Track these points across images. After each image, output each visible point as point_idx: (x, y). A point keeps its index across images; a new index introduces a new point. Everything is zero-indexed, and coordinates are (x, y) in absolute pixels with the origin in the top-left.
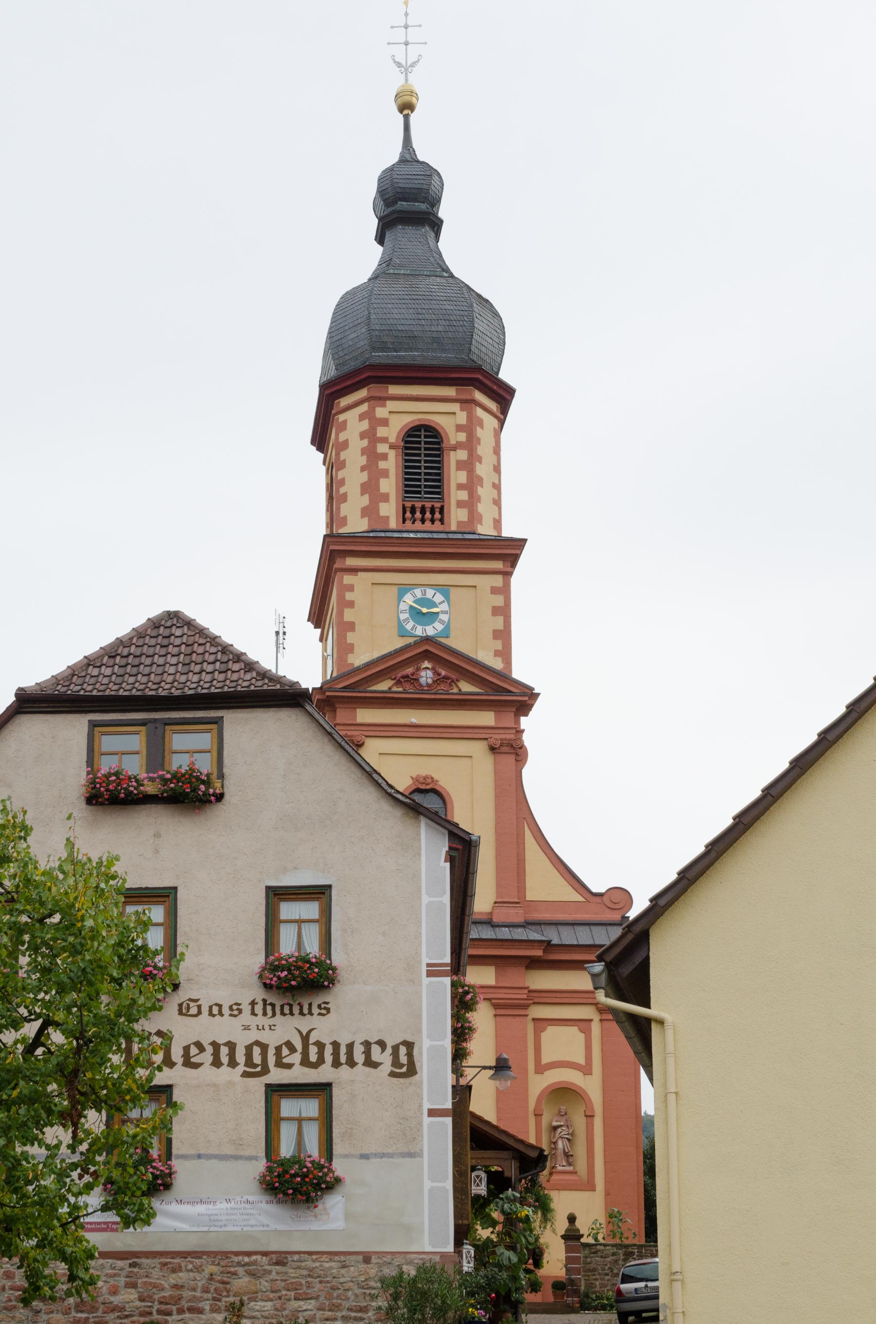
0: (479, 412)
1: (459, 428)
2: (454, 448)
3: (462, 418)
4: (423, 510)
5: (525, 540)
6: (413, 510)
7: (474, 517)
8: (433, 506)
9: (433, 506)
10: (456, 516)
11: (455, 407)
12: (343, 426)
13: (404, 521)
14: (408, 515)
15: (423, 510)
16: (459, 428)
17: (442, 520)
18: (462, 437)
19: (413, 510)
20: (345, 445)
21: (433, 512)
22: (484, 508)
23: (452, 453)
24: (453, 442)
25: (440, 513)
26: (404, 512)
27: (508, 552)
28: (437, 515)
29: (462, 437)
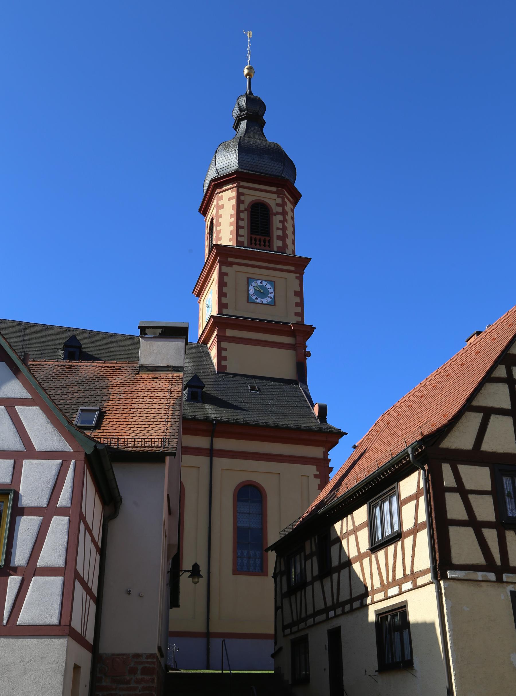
0: (286, 200)
1: (278, 205)
2: (275, 214)
3: (279, 201)
4: (260, 241)
5: (309, 260)
6: (255, 240)
7: (285, 246)
8: (265, 239)
9: (265, 239)
10: (277, 243)
11: (275, 196)
12: (222, 198)
13: (251, 244)
14: (253, 242)
15: (260, 241)
16: (278, 205)
17: (269, 246)
18: (280, 209)
19: (255, 240)
20: (222, 207)
21: (265, 242)
22: (289, 242)
23: (274, 217)
24: (274, 211)
25: (268, 244)
26: (251, 240)
27: (300, 264)
28: (267, 244)
29: (280, 209)
